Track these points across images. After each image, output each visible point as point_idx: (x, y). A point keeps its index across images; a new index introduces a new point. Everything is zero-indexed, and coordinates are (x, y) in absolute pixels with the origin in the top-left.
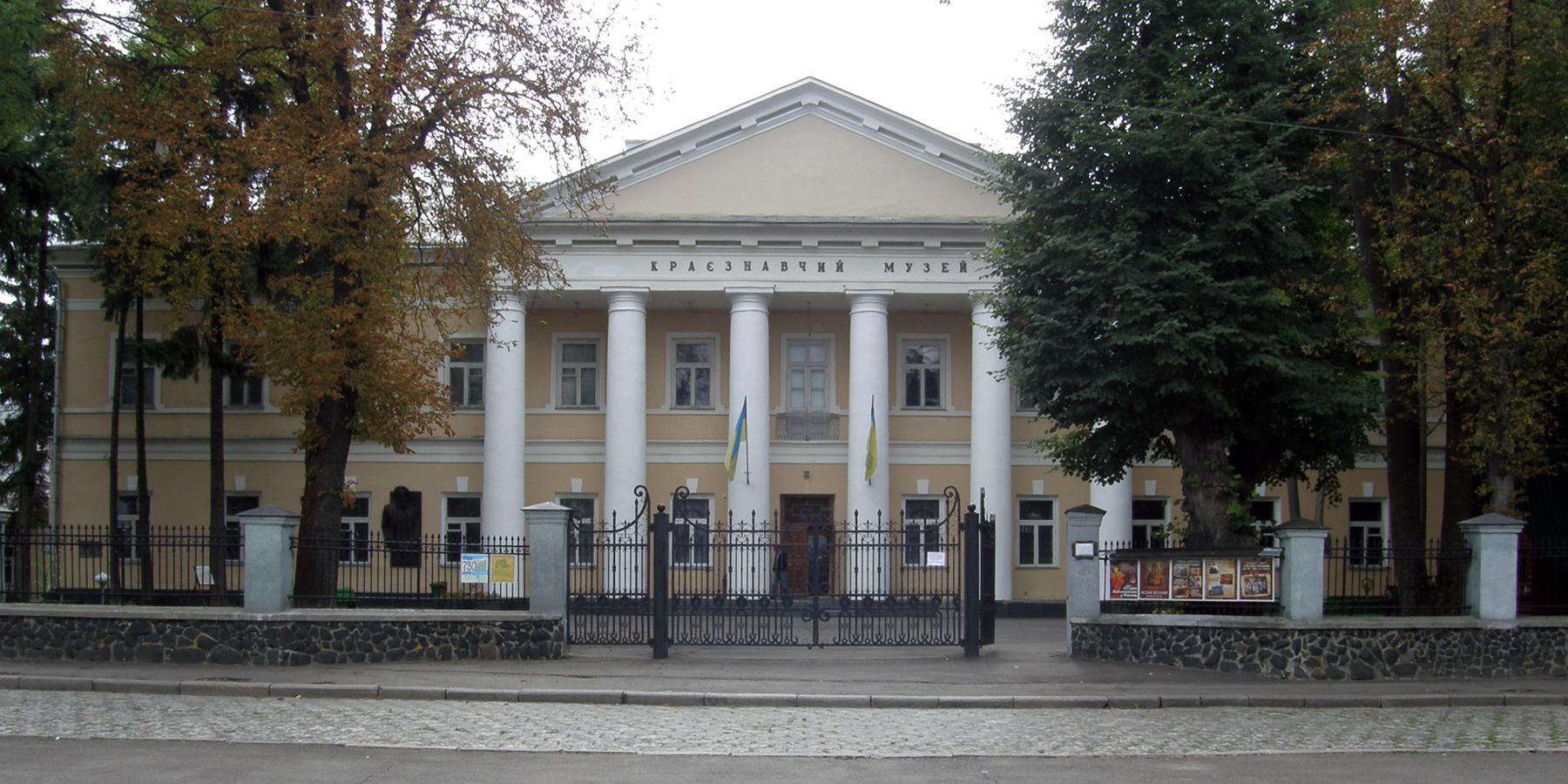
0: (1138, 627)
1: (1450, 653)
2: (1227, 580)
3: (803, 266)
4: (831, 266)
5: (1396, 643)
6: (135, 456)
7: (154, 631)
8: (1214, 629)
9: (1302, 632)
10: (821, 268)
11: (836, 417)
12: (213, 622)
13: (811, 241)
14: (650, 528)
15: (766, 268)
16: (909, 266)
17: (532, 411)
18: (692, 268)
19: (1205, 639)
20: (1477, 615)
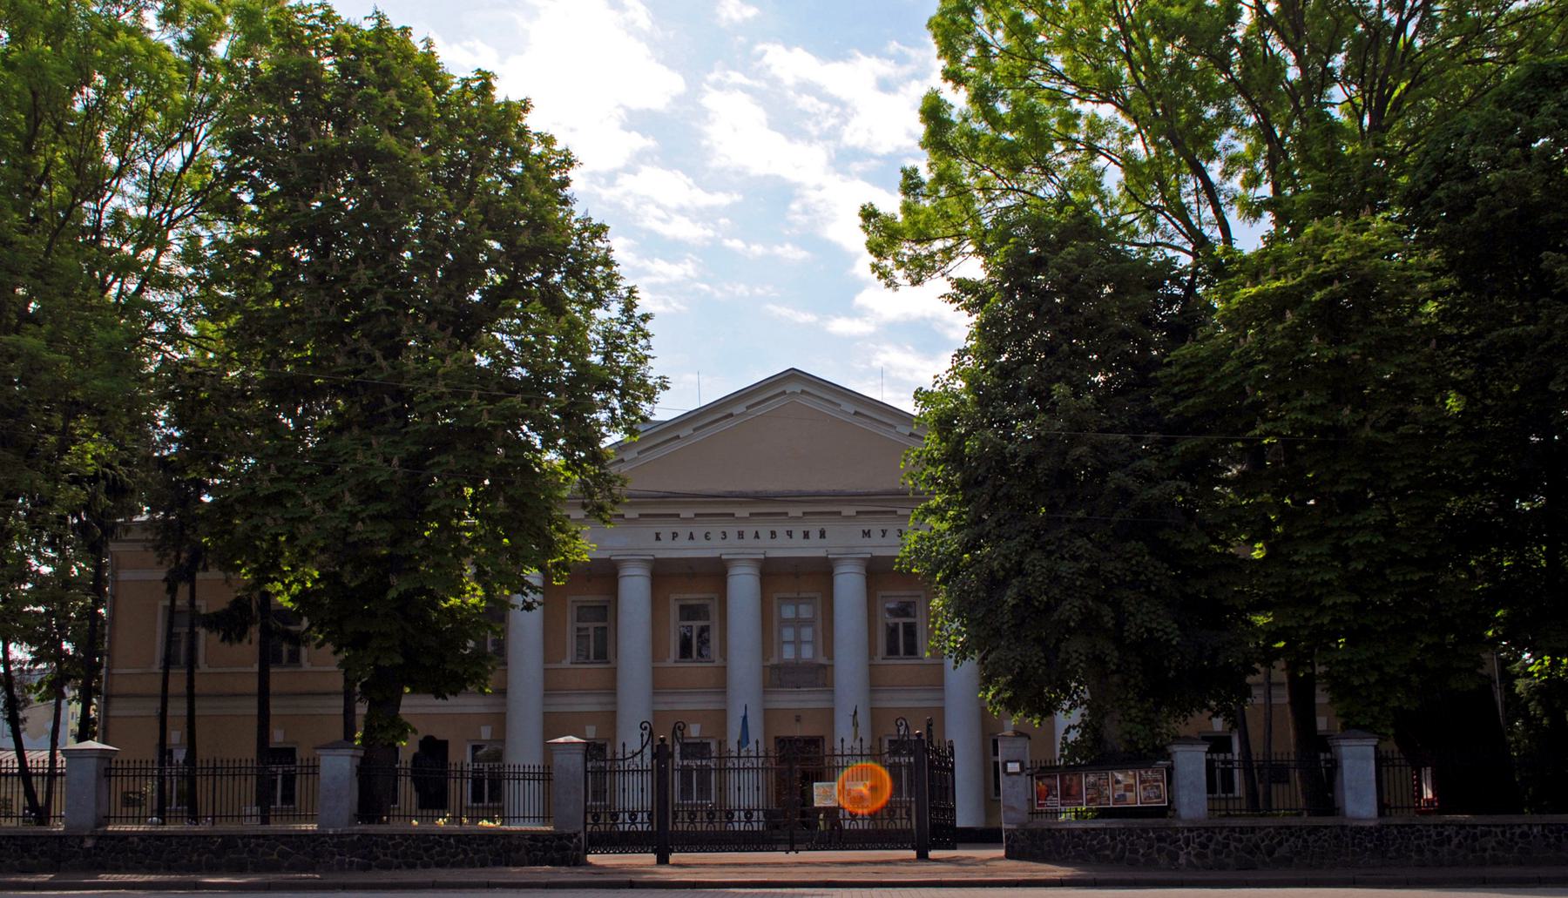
0: (1060, 830)
1: (1323, 847)
2: (1129, 788)
3: (790, 534)
4: (814, 535)
5: (1272, 839)
6: (185, 712)
7: (240, 845)
8: (1120, 829)
9: (1190, 830)
10: (806, 535)
11: (824, 667)
12: (291, 836)
13: (795, 511)
14: (654, 756)
15: (757, 536)
16: (884, 533)
17: (549, 666)
18: (691, 537)
19: (1113, 838)
20: (1344, 815)
